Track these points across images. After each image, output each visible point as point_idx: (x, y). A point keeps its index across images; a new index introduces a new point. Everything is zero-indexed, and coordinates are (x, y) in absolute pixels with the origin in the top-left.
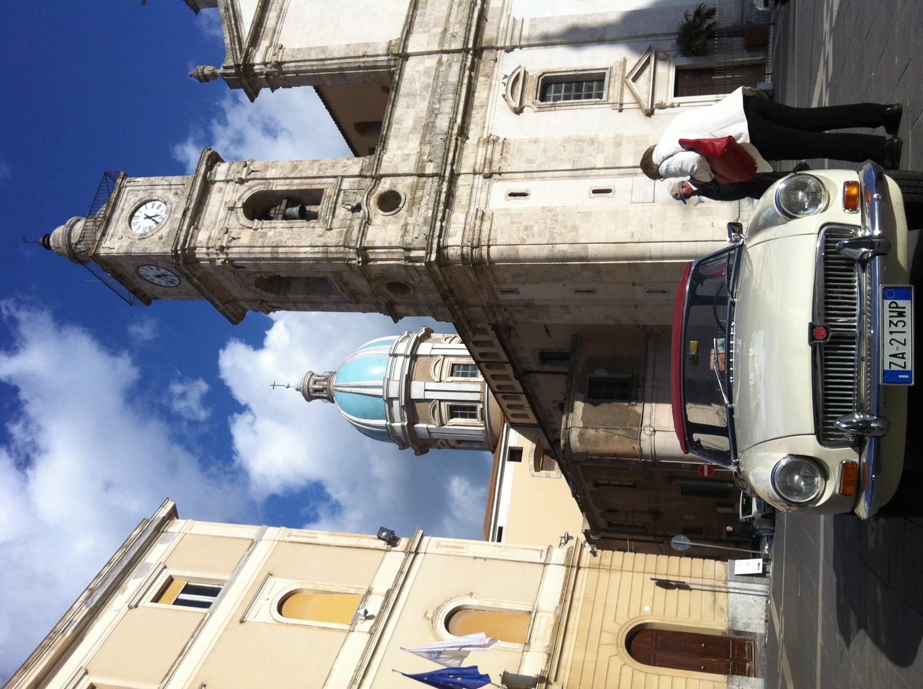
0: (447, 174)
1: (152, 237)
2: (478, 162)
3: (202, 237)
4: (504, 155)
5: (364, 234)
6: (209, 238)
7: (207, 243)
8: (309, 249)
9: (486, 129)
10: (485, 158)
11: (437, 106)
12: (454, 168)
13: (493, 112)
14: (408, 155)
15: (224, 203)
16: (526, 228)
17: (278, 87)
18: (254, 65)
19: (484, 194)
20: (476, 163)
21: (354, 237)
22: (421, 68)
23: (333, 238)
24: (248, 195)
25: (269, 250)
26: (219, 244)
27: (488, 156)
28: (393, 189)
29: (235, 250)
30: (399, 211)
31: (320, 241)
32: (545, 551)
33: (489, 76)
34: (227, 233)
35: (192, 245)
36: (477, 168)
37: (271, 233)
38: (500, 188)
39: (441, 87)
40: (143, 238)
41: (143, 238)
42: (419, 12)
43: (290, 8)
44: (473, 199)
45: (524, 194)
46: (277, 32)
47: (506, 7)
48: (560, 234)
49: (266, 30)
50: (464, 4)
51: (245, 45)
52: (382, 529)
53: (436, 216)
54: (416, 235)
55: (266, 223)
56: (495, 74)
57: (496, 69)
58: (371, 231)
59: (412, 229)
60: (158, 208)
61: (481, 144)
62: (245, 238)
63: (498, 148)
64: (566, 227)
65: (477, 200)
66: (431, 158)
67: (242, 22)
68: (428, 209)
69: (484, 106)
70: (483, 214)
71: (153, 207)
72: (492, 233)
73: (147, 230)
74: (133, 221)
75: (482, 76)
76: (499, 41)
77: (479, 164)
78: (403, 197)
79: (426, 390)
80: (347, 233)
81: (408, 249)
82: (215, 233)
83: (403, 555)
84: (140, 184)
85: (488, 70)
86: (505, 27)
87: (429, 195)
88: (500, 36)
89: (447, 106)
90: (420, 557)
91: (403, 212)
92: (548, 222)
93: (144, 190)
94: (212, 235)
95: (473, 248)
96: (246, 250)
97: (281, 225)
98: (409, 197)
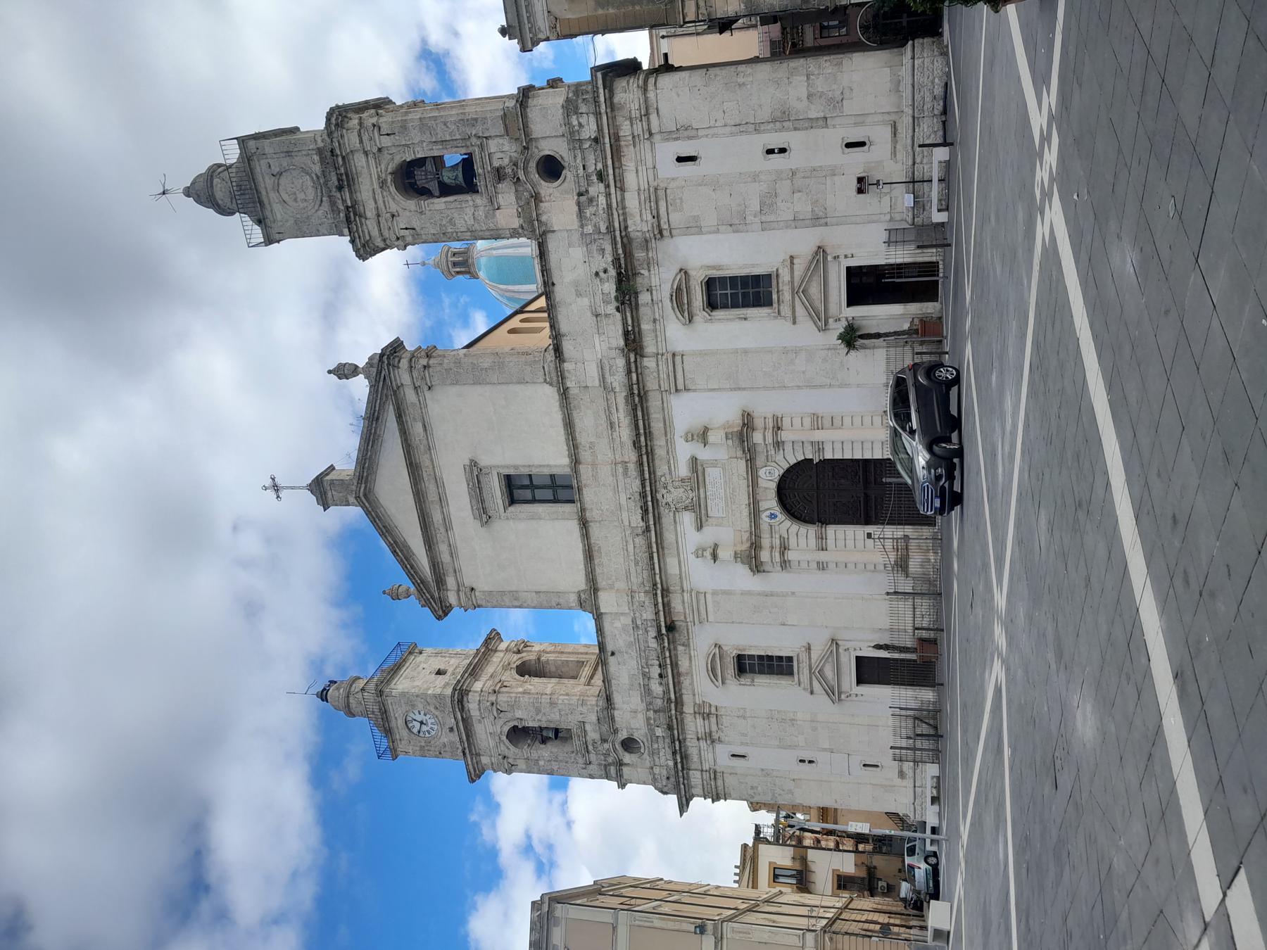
2: (699, 731)
4: (720, 726)
9: (697, 696)
10: (705, 733)
11: (647, 670)
12: (681, 737)
13: (699, 680)
15: (489, 735)
16: (752, 788)
19: (711, 755)
20: (697, 732)
22: (618, 624)
27: (707, 731)
32: (801, 936)
33: (687, 645)
36: (700, 736)
38: (722, 752)
39: (645, 651)
42: (596, 561)
43: (458, 542)
44: (703, 758)
45: (744, 756)
46: (457, 571)
47: (684, 575)
48: (780, 795)
49: (444, 565)
53: (679, 781)
56: (691, 645)
57: (691, 640)
61: (697, 715)
63: (713, 720)
64: (783, 790)
65: (707, 759)
66: (658, 723)
67: (414, 554)
69: (690, 673)
70: (715, 772)
72: (726, 790)
75: (680, 645)
76: (687, 616)
77: (700, 733)
85: (684, 640)
86: (689, 601)
87: (664, 748)
88: (687, 612)
89: (655, 671)
90: (725, 941)
92: (769, 785)
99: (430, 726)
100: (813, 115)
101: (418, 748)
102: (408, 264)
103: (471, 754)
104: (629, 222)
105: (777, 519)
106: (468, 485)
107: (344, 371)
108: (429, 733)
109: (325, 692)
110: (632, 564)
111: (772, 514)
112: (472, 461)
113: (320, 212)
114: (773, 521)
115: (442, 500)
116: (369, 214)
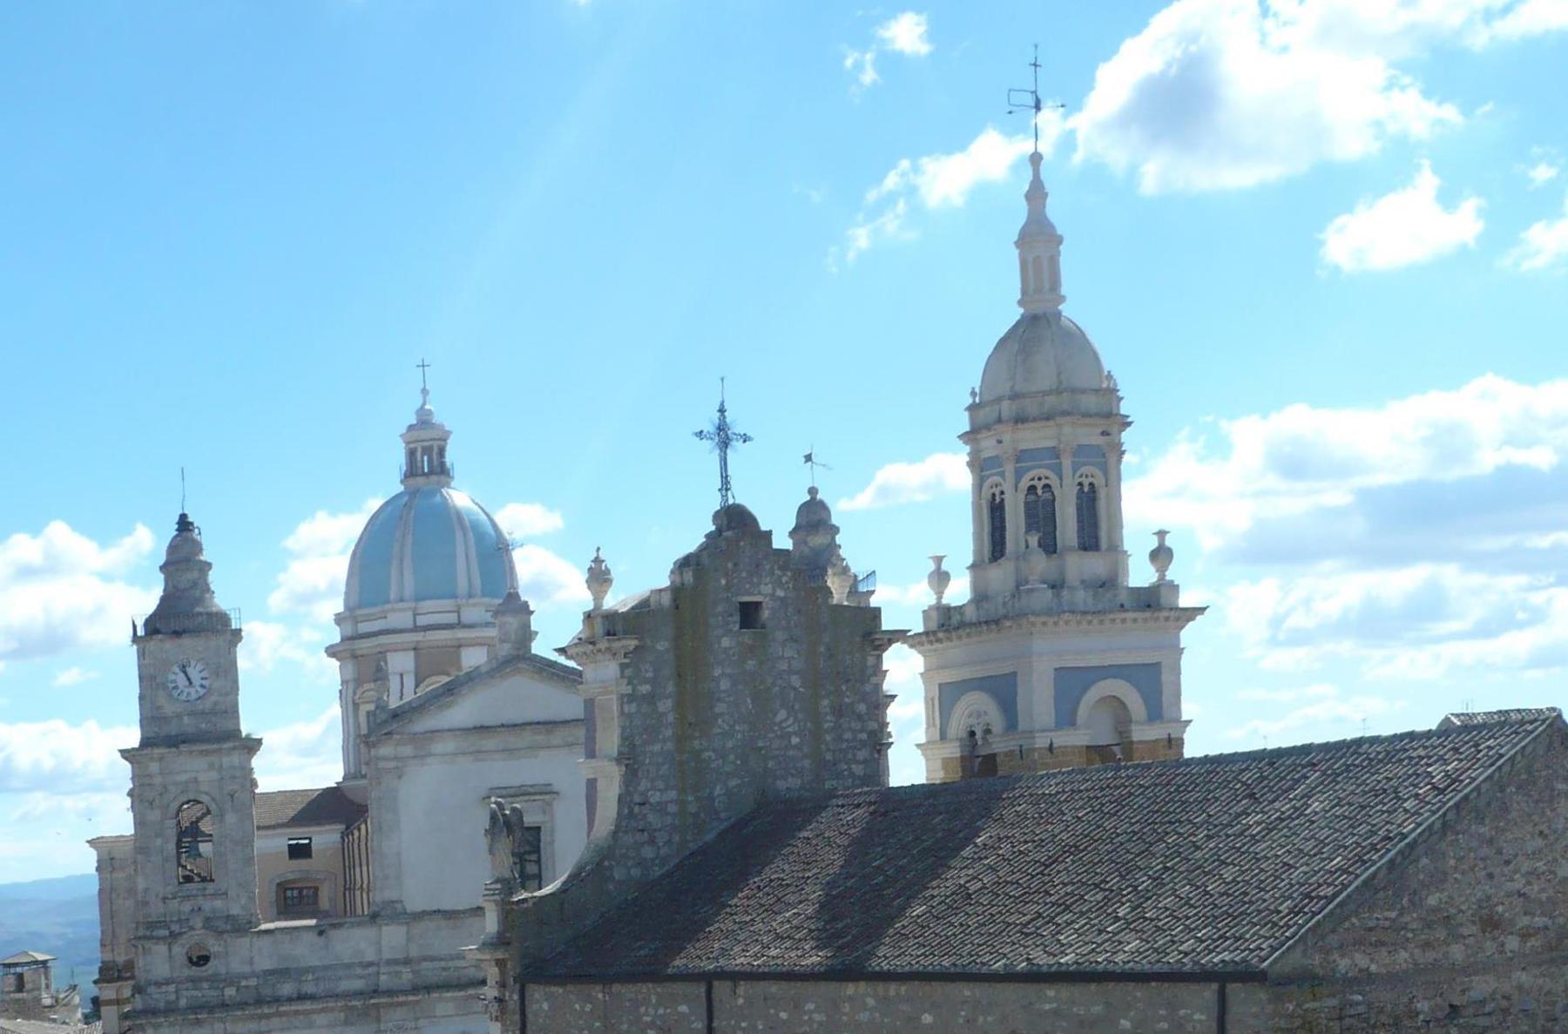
5: (157, 944)
14: (251, 962)
50: (444, 974)
54: (154, 996)
73: (171, 685)
78: (204, 968)
79: (402, 675)
87: (203, 996)
98: (205, 974)
99: (186, 690)
101: (152, 671)
102: (423, 366)
108: (174, 688)
110: (443, 964)
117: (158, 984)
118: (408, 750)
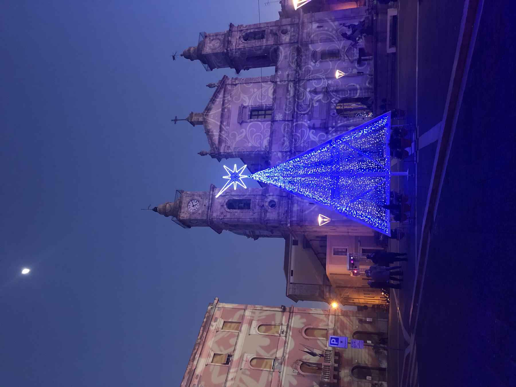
0: (290, 197)
1: (197, 213)
3: (215, 215)
5: (266, 216)
6: (217, 215)
7: (217, 217)
8: (249, 220)
17: (228, 158)
18: (221, 153)
21: (263, 216)
23: (256, 216)
24: (227, 201)
25: (236, 220)
26: (220, 218)
28: (273, 200)
29: (226, 219)
30: (276, 207)
31: (252, 217)
34: (222, 214)
35: (212, 218)
37: (236, 214)
40: (194, 214)
41: (194, 214)
42: (274, 135)
51: (217, 146)
52: (282, 306)
54: (282, 217)
55: (234, 210)
58: (268, 214)
59: (281, 214)
60: (196, 202)
62: (228, 216)
68: (285, 207)
70: (302, 210)
71: (194, 202)
73: (194, 211)
74: (188, 207)
80: (260, 215)
81: (281, 221)
82: (219, 214)
83: (289, 313)
84: (188, 194)
91: (277, 208)
93: (190, 196)
94: (218, 215)
95: (300, 221)
96: (229, 220)
97: (239, 211)
100: (352, 16)
103: (211, 210)
104: (303, 39)
105: (335, 115)
106: (239, 111)
107: (210, 86)
108: (195, 210)
109: (156, 208)
111: (333, 113)
112: (242, 104)
113: (219, 48)
114: (334, 116)
115: (229, 117)
116: (234, 44)
117: (279, 216)
118: (223, 145)
